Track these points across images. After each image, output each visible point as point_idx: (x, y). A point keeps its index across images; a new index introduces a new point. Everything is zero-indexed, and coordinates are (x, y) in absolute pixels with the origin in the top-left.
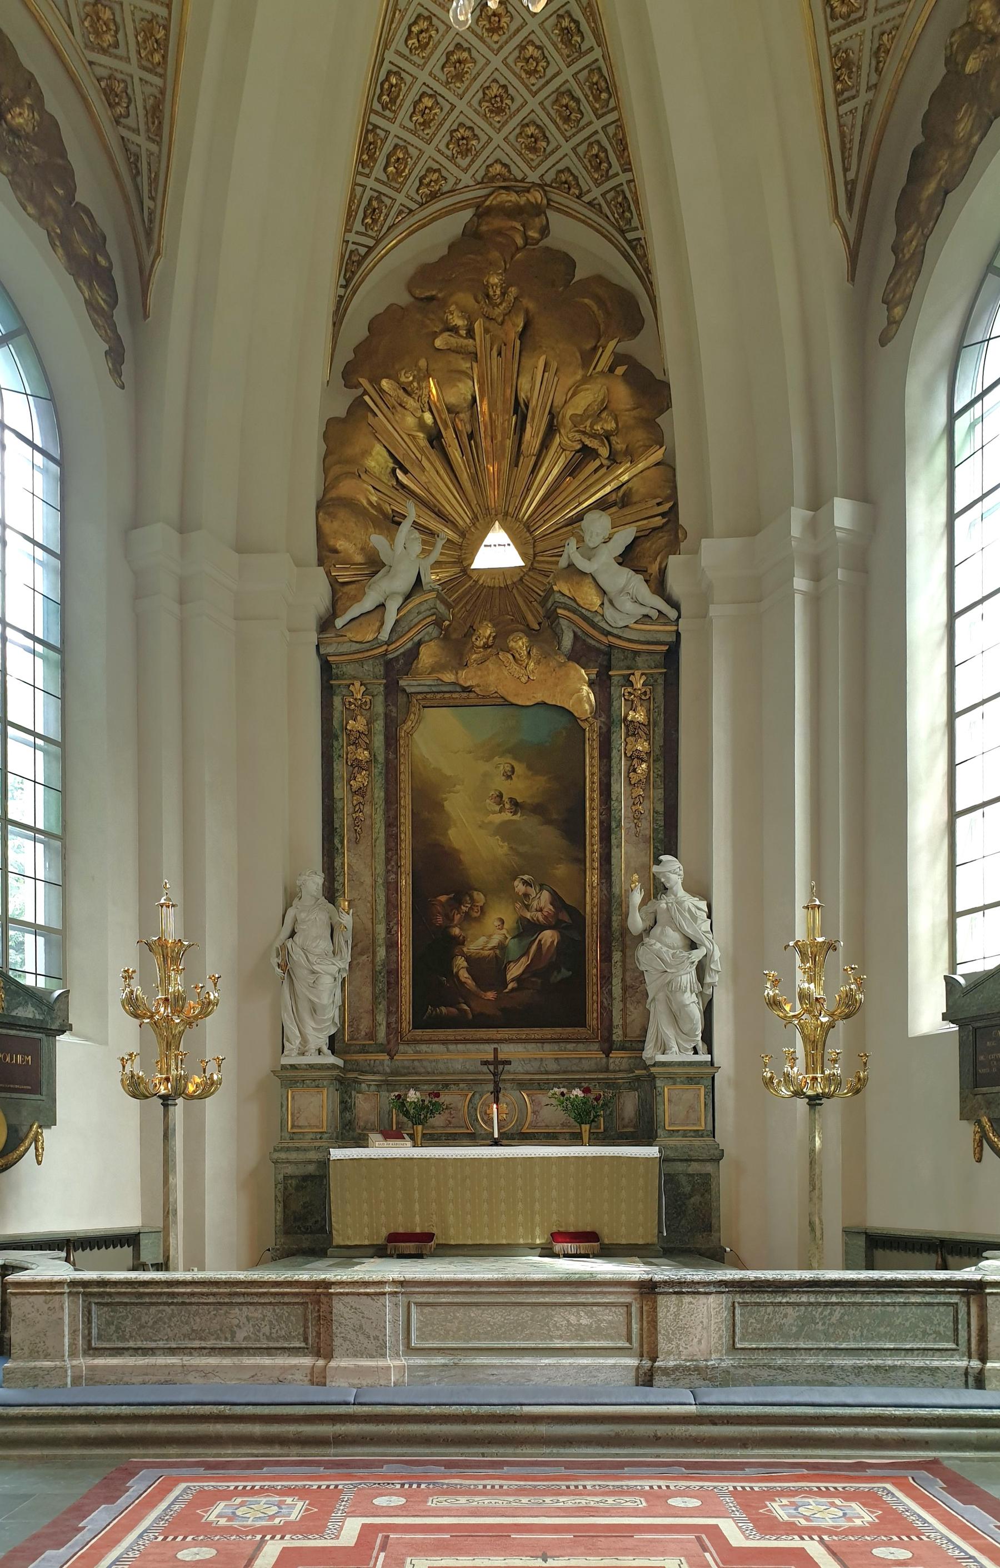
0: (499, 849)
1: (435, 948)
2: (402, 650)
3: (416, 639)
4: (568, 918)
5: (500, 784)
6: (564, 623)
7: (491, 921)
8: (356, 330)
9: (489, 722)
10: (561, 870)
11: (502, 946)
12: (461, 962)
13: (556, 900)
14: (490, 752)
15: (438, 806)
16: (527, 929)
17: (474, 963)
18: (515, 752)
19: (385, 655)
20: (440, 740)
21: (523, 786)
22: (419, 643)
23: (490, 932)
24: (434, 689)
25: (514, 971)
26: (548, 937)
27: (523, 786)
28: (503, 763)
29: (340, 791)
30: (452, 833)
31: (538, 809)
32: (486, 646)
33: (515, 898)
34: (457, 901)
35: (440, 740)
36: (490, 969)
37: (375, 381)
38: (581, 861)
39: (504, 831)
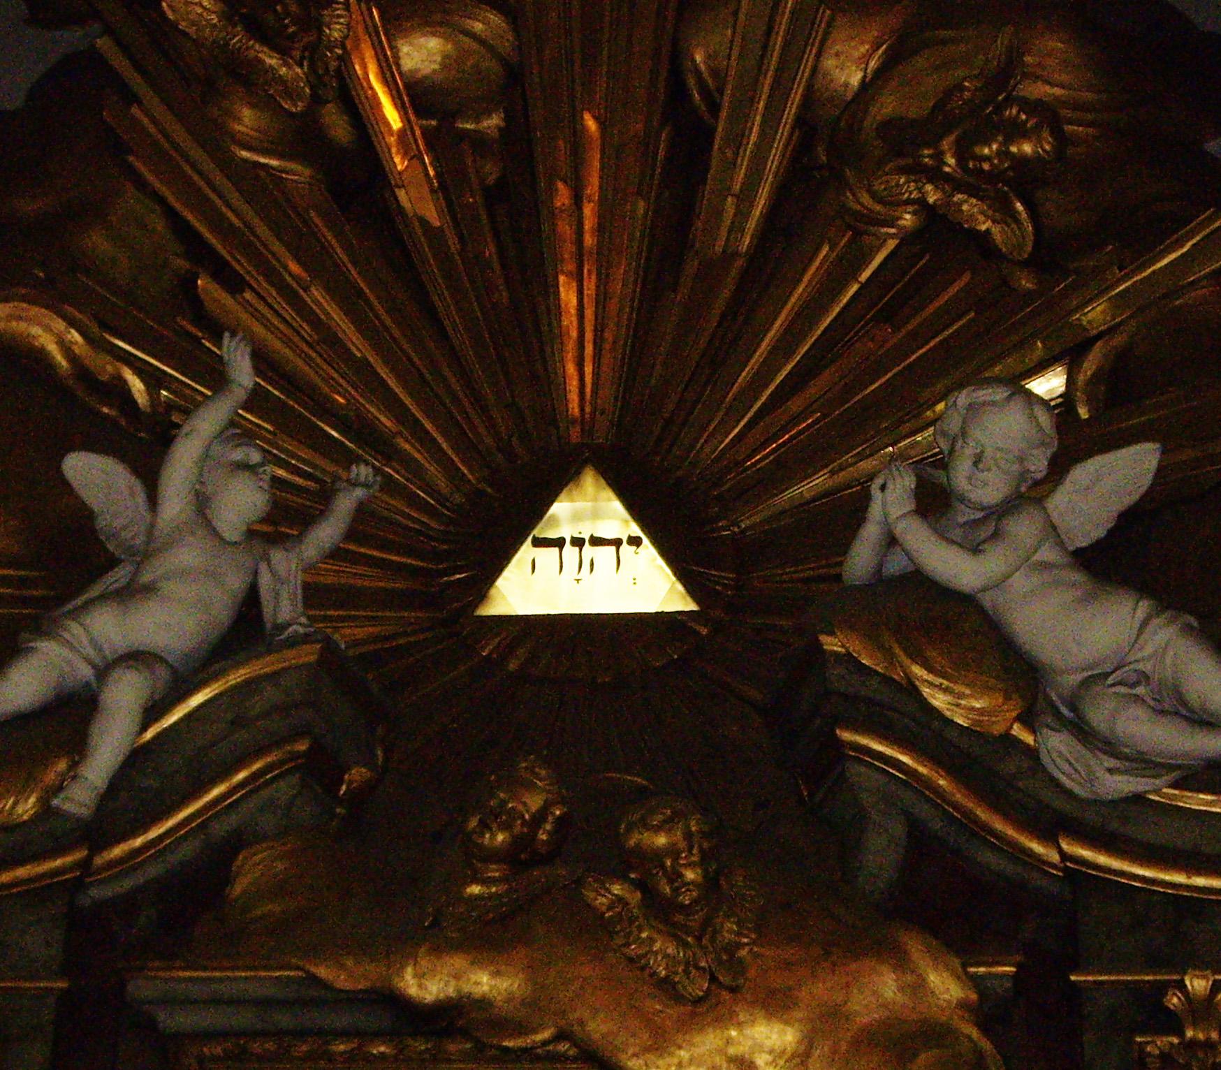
2: (153, 871)
3: (220, 829)
6: (856, 772)
19: (78, 885)
22: (237, 842)
24: (284, 1019)
32: (520, 857)
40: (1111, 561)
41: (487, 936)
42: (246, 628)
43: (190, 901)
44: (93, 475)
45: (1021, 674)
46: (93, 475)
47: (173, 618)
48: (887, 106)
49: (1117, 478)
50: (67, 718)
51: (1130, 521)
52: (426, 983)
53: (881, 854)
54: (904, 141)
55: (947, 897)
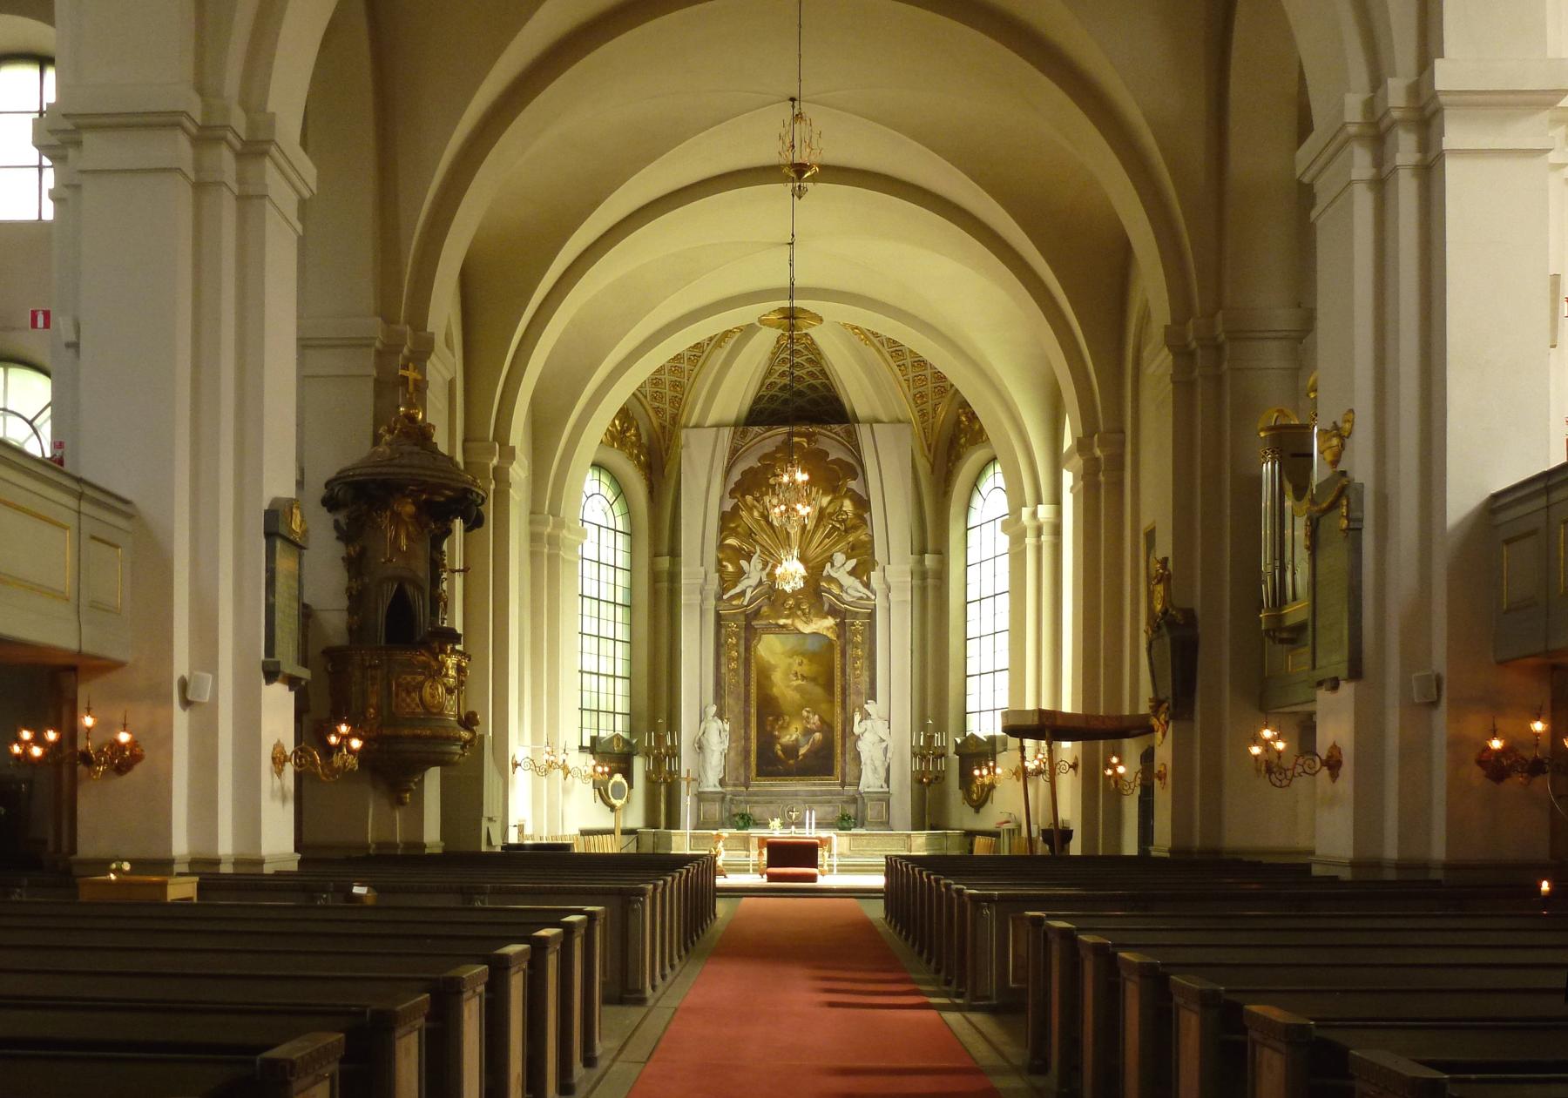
0: (797, 696)
1: (767, 742)
4: (827, 726)
5: (796, 668)
7: (793, 729)
8: (736, 476)
9: (791, 641)
10: (824, 706)
13: (821, 719)
14: (793, 653)
15: (768, 678)
16: (808, 733)
17: (785, 749)
18: (803, 654)
20: (770, 648)
21: (806, 669)
23: (791, 735)
25: (802, 751)
27: (806, 669)
28: (798, 659)
30: (775, 690)
31: (814, 680)
33: (802, 718)
34: (777, 720)
35: (770, 648)
36: (791, 750)
37: (743, 496)
38: (832, 702)
39: (797, 688)
40: (852, 573)
41: (787, 617)
42: (761, 582)
43: (757, 614)
44: (743, 563)
45: (841, 586)
46: (743, 563)
47: (753, 581)
48: (829, 510)
49: (853, 562)
50: (743, 593)
51: (854, 569)
52: (782, 622)
53: (826, 607)
54: (831, 515)
55: (833, 612)
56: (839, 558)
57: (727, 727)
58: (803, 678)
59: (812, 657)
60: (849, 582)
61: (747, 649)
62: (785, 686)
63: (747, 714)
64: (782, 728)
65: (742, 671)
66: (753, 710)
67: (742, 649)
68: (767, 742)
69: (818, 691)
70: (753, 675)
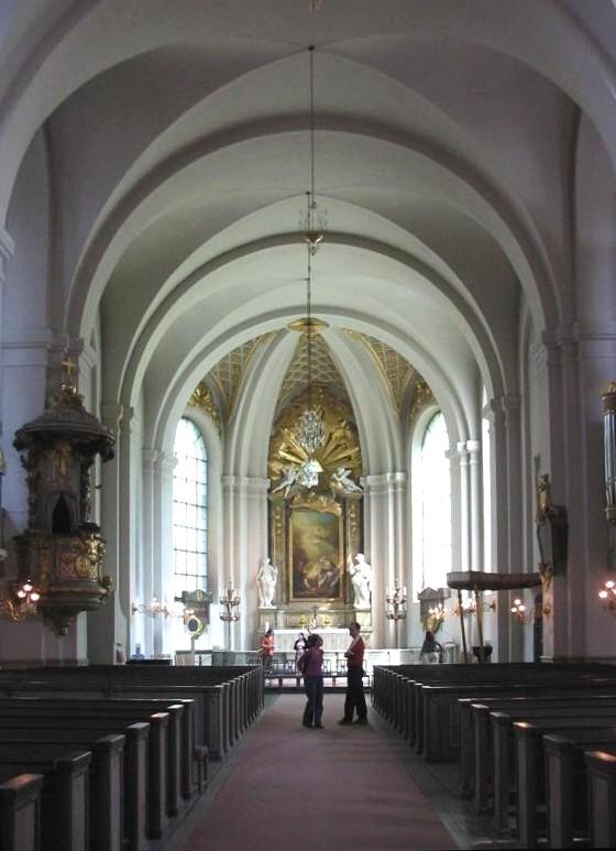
1: (299, 577)
5: (316, 532)
7: (314, 570)
9: (314, 516)
11: (317, 577)
12: (306, 581)
16: (324, 571)
17: (309, 581)
18: (320, 524)
20: (300, 521)
21: (323, 533)
23: (314, 572)
25: (320, 583)
26: (329, 574)
27: (323, 533)
29: (274, 535)
31: (327, 539)
34: (305, 564)
36: (313, 582)
39: (318, 545)
53: (334, 496)
56: (342, 471)
57: (276, 571)
58: (321, 538)
59: (324, 525)
60: (348, 482)
61: (287, 521)
62: (311, 545)
63: (287, 560)
64: (308, 569)
65: (284, 536)
66: (291, 559)
67: (284, 521)
68: (299, 577)
69: (330, 547)
70: (291, 537)
